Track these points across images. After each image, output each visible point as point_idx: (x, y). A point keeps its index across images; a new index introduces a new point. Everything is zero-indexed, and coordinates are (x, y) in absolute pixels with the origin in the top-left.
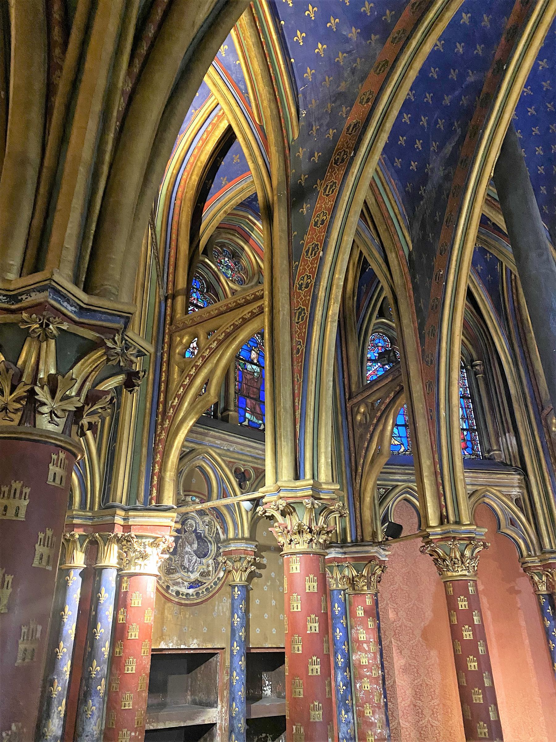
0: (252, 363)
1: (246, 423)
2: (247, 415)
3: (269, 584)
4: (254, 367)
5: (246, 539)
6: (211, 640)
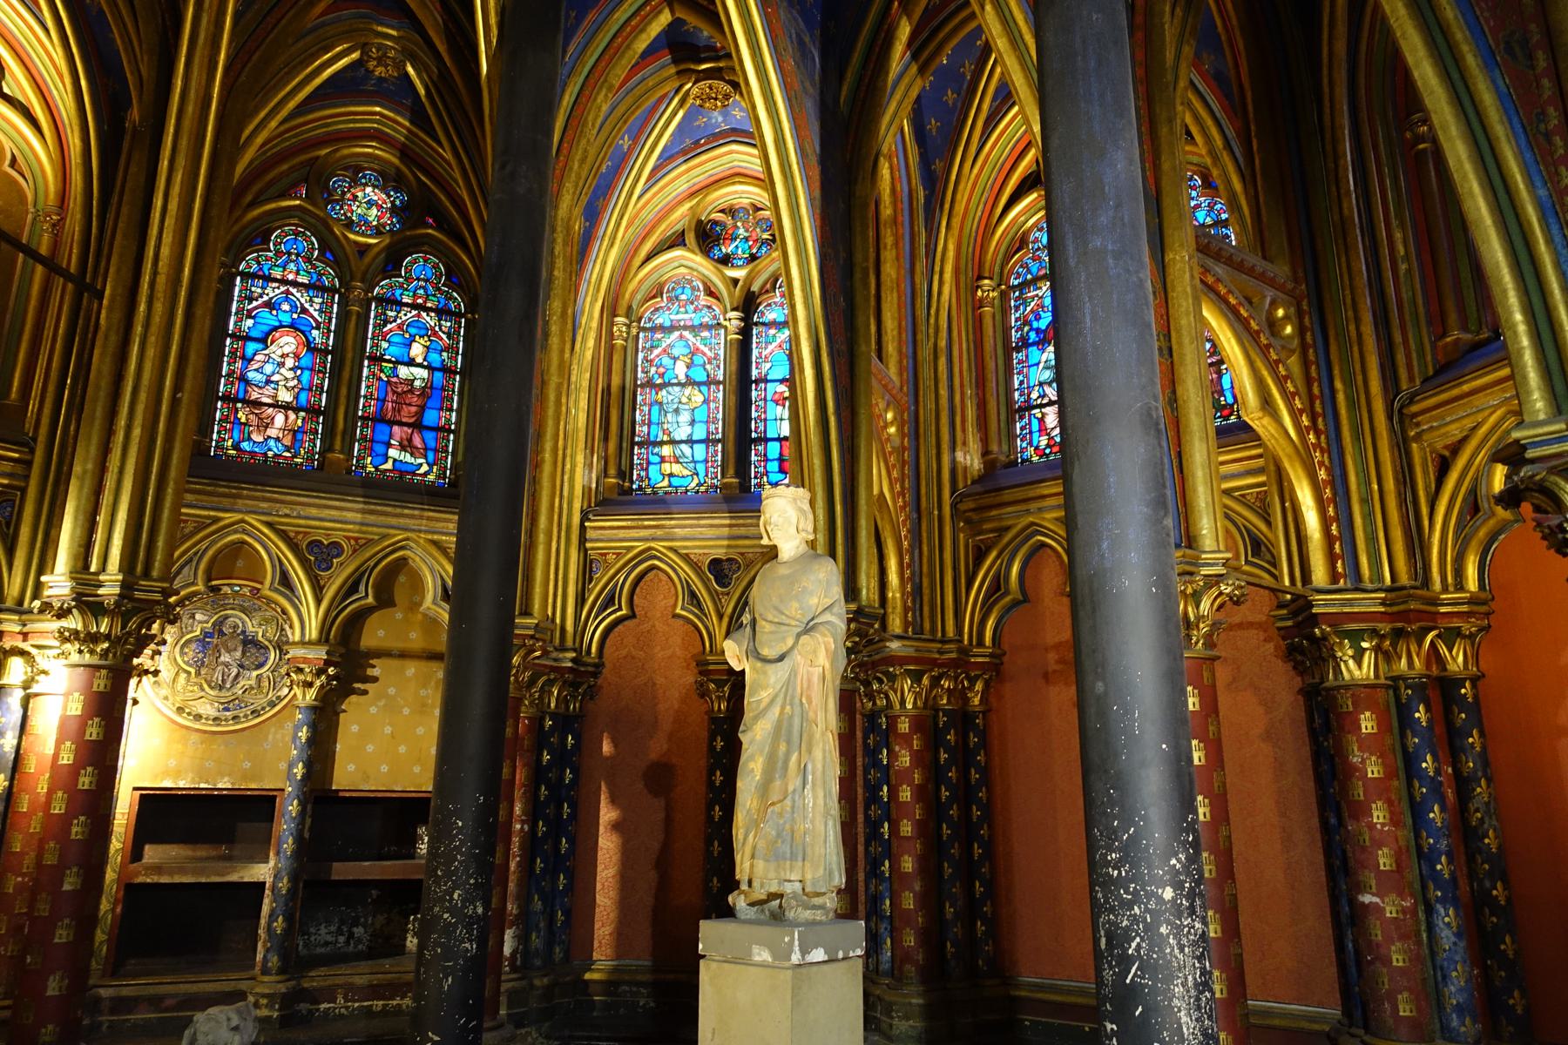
0: (411, 363)
1: (389, 465)
2: (393, 453)
3: (382, 703)
4: (414, 370)
5: (310, 643)
6: (252, 780)
